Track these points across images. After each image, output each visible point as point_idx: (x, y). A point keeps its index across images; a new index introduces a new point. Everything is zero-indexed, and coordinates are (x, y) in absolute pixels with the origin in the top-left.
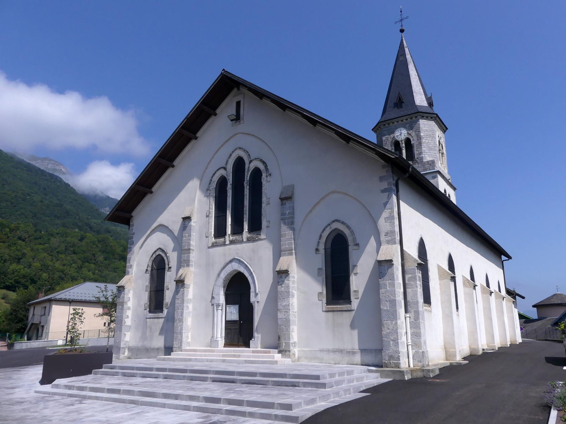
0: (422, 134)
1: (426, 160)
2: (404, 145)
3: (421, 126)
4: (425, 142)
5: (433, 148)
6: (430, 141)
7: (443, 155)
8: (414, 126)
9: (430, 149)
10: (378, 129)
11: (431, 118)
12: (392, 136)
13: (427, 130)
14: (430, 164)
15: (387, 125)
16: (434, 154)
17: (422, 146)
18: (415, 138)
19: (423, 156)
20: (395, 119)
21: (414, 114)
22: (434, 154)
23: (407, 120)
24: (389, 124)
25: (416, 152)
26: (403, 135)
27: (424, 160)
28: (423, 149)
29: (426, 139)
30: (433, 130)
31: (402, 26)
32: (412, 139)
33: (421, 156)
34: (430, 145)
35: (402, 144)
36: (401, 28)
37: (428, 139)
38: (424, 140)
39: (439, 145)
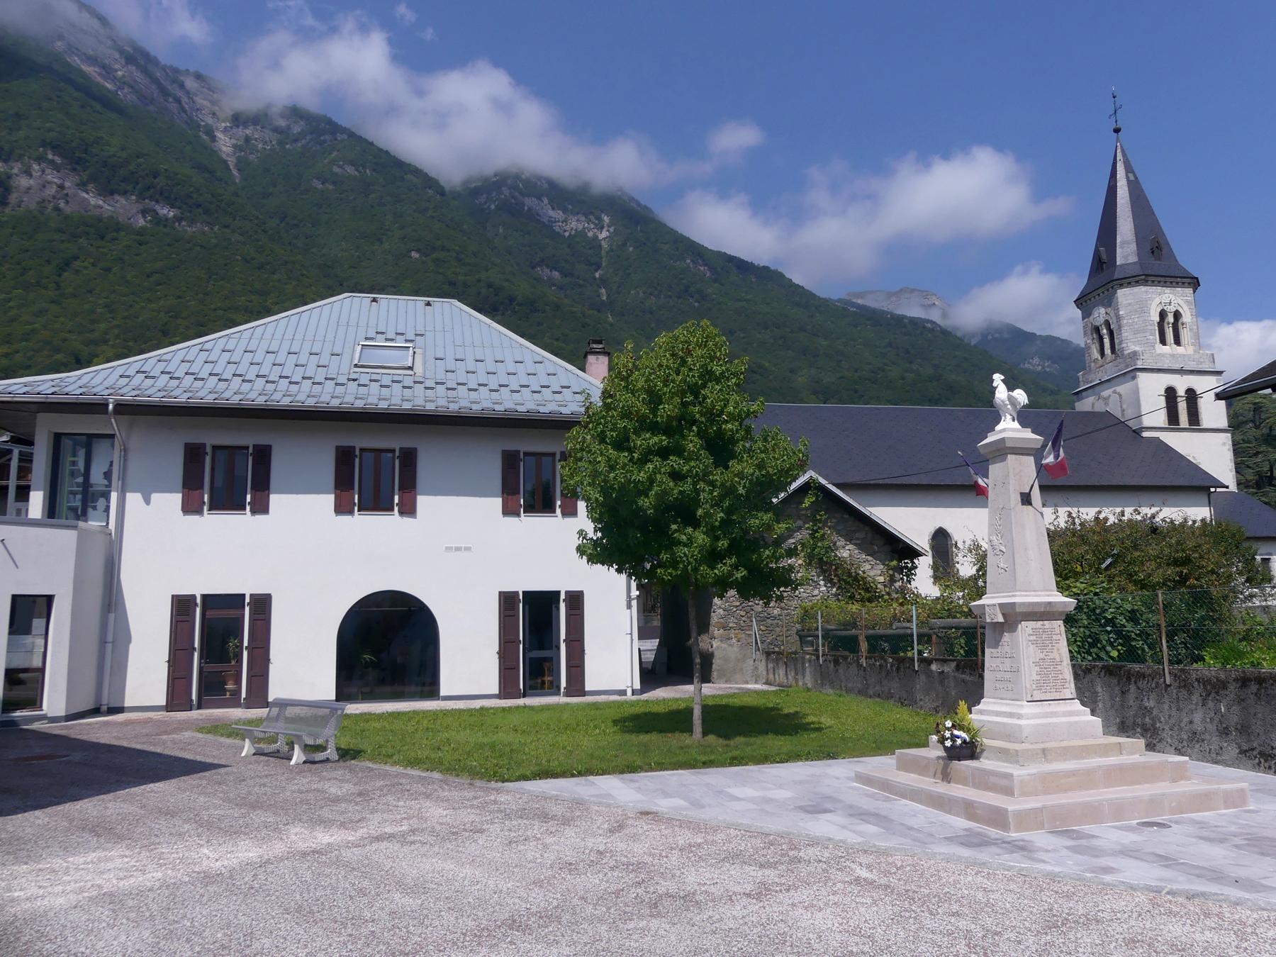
1: (1129, 351)
3: (1120, 300)
9: (1137, 332)
11: (1137, 282)
13: (1130, 304)
18: (1114, 319)
19: (1124, 345)
26: (1101, 316)
36: (1114, 126)
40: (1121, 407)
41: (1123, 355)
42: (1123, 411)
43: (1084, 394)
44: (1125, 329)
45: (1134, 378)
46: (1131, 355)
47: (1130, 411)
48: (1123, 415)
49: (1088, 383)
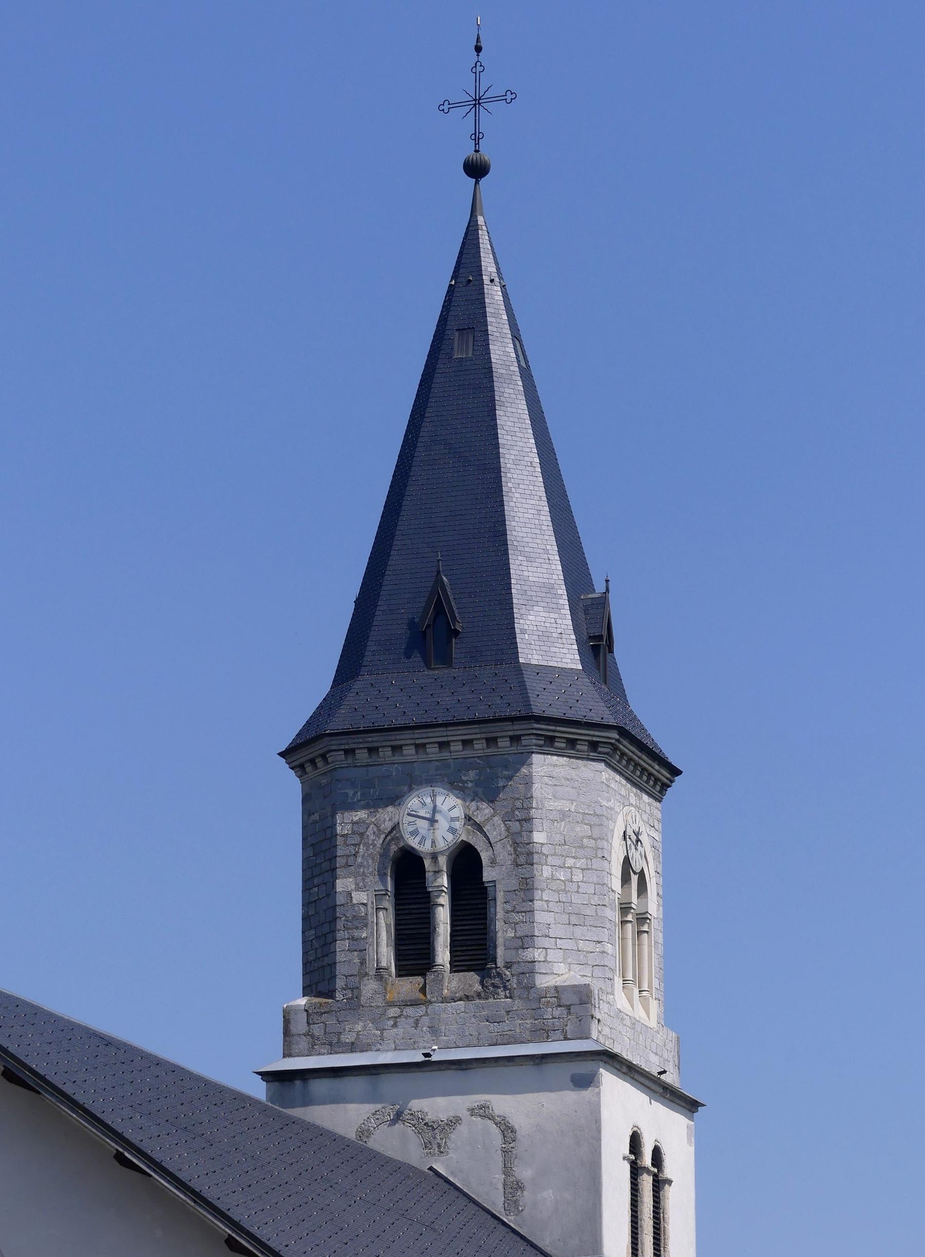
0: (539, 837)
2: (444, 881)
3: (537, 790)
4: (553, 878)
5: (589, 911)
6: (578, 876)
7: (645, 928)
8: (504, 787)
10: (312, 762)
11: (594, 746)
12: (387, 816)
13: (564, 815)
14: (568, 1007)
15: (362, 756)
16: (590, 947)
17: (537, 904)
18: (504, 853)
19: (538, 955)
20: (407, 734)
21: (507, 726)
22: (590, 947)
23: (466, 743)
24: (372, 750)
25: (503, 933)
26: (443, 824)
27: (544, 982)
28: (540, 917)
29: (557, 861)
30: (595, 815)
31: (477, 138)
32: (490, 853)
33: (529, 954)
34: (576, 899)
35: (437, 872)
36: (467, 151)
37: (570, 862)
38: (546, 872)
39: (626, 879)
40: (507, 1170)
41: (531, 987)
42: (513, 1188)
43: (319, 1086)
44: (544, 898)
45: (586, 1082)
46: (568, 999)
47: (548, 1194)
48: (512, 1202)
49: (335, 1047)
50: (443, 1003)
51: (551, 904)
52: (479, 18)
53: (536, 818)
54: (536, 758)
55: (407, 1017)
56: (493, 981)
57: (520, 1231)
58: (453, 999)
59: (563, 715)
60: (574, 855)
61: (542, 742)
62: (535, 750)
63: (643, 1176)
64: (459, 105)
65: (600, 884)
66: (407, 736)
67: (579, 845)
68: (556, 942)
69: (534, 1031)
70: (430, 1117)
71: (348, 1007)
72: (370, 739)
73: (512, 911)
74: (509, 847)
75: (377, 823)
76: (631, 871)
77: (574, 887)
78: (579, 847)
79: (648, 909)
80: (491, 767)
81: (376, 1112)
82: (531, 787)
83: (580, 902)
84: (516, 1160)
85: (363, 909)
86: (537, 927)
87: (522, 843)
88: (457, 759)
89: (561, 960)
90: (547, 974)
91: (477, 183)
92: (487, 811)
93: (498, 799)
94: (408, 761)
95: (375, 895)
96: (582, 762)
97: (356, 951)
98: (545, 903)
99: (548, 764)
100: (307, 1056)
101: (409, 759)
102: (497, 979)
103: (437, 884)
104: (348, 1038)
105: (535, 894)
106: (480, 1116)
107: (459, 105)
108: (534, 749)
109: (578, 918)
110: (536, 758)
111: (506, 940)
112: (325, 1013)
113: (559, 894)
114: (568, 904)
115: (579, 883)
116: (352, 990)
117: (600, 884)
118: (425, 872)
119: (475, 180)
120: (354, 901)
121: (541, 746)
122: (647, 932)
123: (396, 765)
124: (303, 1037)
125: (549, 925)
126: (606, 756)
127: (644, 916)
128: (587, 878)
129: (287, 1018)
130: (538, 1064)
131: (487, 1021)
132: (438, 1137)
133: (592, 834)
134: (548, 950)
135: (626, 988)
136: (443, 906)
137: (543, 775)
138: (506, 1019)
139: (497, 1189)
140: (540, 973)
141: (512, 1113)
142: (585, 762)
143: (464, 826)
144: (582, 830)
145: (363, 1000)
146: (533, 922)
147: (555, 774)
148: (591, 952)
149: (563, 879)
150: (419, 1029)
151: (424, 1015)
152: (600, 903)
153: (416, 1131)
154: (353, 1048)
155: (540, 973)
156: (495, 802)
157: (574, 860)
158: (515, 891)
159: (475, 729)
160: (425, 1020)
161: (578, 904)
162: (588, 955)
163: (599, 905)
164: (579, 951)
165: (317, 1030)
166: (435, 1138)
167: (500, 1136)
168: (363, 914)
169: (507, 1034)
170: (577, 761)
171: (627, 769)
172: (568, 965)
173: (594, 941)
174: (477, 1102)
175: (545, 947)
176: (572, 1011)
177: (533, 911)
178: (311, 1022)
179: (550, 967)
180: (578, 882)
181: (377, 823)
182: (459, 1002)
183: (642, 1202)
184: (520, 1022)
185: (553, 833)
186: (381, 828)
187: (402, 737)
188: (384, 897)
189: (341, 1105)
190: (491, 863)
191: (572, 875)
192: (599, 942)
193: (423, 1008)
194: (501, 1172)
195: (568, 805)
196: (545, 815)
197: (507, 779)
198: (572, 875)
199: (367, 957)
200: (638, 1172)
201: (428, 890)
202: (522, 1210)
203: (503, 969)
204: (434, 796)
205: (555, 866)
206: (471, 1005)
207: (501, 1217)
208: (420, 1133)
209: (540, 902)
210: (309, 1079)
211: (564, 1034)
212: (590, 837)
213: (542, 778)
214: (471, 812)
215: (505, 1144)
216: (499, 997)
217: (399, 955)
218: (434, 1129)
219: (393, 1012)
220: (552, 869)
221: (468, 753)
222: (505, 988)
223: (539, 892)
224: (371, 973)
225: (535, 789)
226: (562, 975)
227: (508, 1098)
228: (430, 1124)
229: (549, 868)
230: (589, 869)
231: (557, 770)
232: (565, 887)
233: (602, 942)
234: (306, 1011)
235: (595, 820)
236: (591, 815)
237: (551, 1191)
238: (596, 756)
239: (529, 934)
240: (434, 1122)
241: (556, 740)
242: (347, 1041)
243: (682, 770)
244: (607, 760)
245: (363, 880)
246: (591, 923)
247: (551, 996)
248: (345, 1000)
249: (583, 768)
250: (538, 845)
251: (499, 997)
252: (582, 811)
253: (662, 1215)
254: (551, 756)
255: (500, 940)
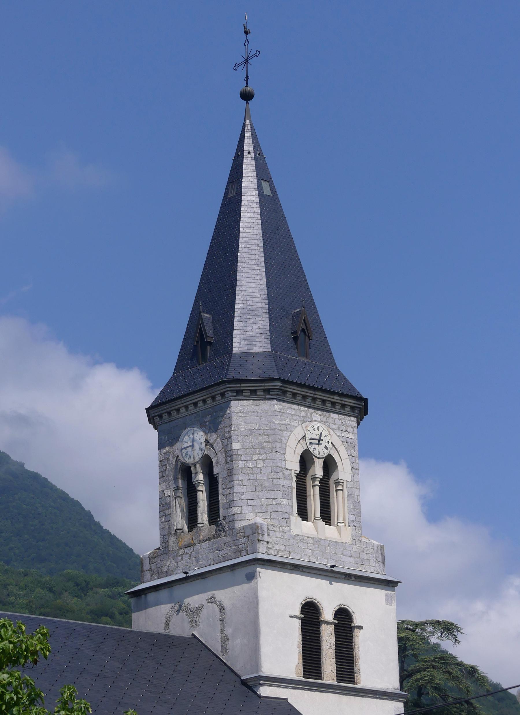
0: (236, 446)
1: (244, 523)
3: (235, 420)
4: (245, 467)
6: (261, 464)
7: (340, 487)
8: (221, 421)
11: (267, 391)
13: (251, 432)
14: (248, 537)
16: (269, 502)
17: (235, 482)
19: (236, 510)
20: (179, 402)
21: (217, 388)
22: (269, 502)
26: (197, 447)
28: (237, 489)
29: (247, 457)
30: (271, 429)
32: (216, 459)
34: (259, 477)
36: (242, 86)
37: (255, 457)
40: (222, 631)
41: (233, 528)
42: (225, 639)
43: (151, 597)
44: (240, 478)
45: (251, 577)
46: (248, 532)
48: (224, 648)
49: (160, 574)
50: (200, 543)
51: (244, 482)
52: (246, 16)
53: (234, 436)
54: (233, 403)
55: (187, 553)
56: (219, 528)
57: (227, 664)
58: (203, 541)
59: (269, 377)
60: (258, 453)
61: (235, 394)
62: (232, 399)
63: (322, 625)
64: (240, 64)
65: (274, 467)
66: (179, 403)
67: (261, 447)
68: (248, 502)
69: (235, 552)
70: (192, 607)
71: (164, 552)
72: (165, 407)
73: (225, 488)
74: (223, 453)
75: (173, 451)
76: (314, 457)
77: (258, 470)
78: (261, 448)
79: (338, 477)
80: (216, 412)
81: (172, 607)
82: (231, 420)
83: (262, 478)
84: (225, 624)
85: (169, 499)
86: (235, 495)
87: (228, 451)
88: (202, 410)
89: (251, 512)
90: (242, 520)
91: (247, 103)
92: (214, 436)
93: (219, 429)
94: (184, 416)
95: (174, 490)
96: (262, 401)
97: (167, 522)
98: (240, 482)
99: (241, 405)
100: (150, 581)
101: (184, 414)
102: (221, 527)
103: (196, 480)
104: (165, 569)
105: (234, 477)
106: (211, 602)
107: (240, 64)
108: (232, 398)
109: (261, 487)
110: (233, 403)
111: (223, 504)
112: (156, 557)
113: (249, 475)
114: (254, 480)
115: (262, 468)
116: (165, 543)
117: (274, 467)
118: (192, 474)
119: (246, 102)
120: (166, 495)
121: (235, 396)
122: (342, 490)
123: (180, 419)
124: (148, 571)
125: (243, 493)
126: (277, 396)
127: (338, 481)
128: (266, 465)
129: (142, 562)
130: (232, 570)
131: (217, 550)
132: (195, 617)
133: (269, 440)
134: (243, 507)
135: (315, 522)
136: (202, 491)
137: (238, 411)
138: (224, 548)
139: (218, 642)
140: (238, 520)
141: (223, 599)
142: (264, 401)
143: (205, 446)
144: (263, 439)
145: (170, 548)
146: (233, 493)
147: (245, 410)
148: (269, 505)
149: (252, 467)
150: (191, 559)
151: (193, 552)
152: (275, 477)
153: (187, 615)
154: (167, 574)
155: (238, 520)
156: (218, 430)
157: (258, 455)
158: (226, 477)
159: (204, 393)
160: (193, 555)
161: (261, 479)
162: (268, 507)
163: (274, 478)
164: (262, 505)
165: (153, 567)
166: (194, 618)
167: (219, 612)
168: (169, 502)
169: (225, 556)
170: (259, 401)
171: (306, 402)
172: (255, 514)
173: (271, 499)
174: (209, 595)
175: (241, 505)
176: (250, 539)
177: (233, 487)
178: (151, 563)
179: (244, 516)
180: (261, 467)
181: (173, 451)
182: (206, 542)
183: (322, 640)
184: (230, 548)
185: (245, 442)
186: (175, 454)
187: (178, 403)
188: (178, 491)
189: (159, 606)
190: (217, 464)
191: (257, 464)
192: (275, 499)
193: (192, 547)
194: (220, 632)
195: (254, 426)
196: (239, 433)
197: (221, 417)
198: (257, 464)
199: (171, 524)
200: (320, 624)
201: (193, 483)
202: (228, 652)
203: (222, 521)
204: (193, 433)
205: (247, 460)
206: (210, 543)
207: (220, 657)
208: (188, 616)
209: (237, 481)
210: (146, 594)
211: (247, 552)
212: (267, 442)
213: (237, 414)
214: (208, 438)
215: (221, 616)
216: (222, 536)
217: (190, 521)
218: (194, 613)
219: (181, 552)
220: (245, 462)
221: (206, 406)
222: (224, 530)
223: (237, 476)
224: (172, 533)
225: (233, 420)
226: (252, 519)
227: (222, 591)
228: (192, 610)
229: (243, 462)
230: (267, 459)
231: (247, 408)
232: (253, 471)
233: (276, 498)
234: (149, 557)
235: (271, 432)
236: (269, 429)
237: (239, 640)
238: (256, 398)
239: (232, 499)
240: (193, 609)
241: (257, 391)
242: (164, 570)
243: (366, 398)
244: (277, 398)
245: (169, 483)
246: (269, 489)
247: (241, 532)
248: (163, 549)
249: (263, 405)
250: (235, 450)
251: (222, 536)
252: (263, 428)
253: (354, 646)
254: (242, 401)
255: (221, 505)
